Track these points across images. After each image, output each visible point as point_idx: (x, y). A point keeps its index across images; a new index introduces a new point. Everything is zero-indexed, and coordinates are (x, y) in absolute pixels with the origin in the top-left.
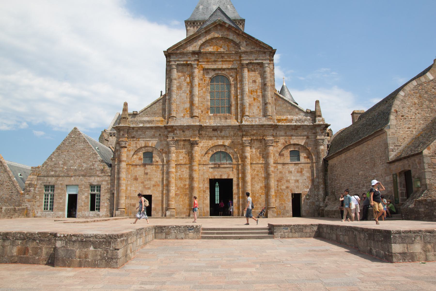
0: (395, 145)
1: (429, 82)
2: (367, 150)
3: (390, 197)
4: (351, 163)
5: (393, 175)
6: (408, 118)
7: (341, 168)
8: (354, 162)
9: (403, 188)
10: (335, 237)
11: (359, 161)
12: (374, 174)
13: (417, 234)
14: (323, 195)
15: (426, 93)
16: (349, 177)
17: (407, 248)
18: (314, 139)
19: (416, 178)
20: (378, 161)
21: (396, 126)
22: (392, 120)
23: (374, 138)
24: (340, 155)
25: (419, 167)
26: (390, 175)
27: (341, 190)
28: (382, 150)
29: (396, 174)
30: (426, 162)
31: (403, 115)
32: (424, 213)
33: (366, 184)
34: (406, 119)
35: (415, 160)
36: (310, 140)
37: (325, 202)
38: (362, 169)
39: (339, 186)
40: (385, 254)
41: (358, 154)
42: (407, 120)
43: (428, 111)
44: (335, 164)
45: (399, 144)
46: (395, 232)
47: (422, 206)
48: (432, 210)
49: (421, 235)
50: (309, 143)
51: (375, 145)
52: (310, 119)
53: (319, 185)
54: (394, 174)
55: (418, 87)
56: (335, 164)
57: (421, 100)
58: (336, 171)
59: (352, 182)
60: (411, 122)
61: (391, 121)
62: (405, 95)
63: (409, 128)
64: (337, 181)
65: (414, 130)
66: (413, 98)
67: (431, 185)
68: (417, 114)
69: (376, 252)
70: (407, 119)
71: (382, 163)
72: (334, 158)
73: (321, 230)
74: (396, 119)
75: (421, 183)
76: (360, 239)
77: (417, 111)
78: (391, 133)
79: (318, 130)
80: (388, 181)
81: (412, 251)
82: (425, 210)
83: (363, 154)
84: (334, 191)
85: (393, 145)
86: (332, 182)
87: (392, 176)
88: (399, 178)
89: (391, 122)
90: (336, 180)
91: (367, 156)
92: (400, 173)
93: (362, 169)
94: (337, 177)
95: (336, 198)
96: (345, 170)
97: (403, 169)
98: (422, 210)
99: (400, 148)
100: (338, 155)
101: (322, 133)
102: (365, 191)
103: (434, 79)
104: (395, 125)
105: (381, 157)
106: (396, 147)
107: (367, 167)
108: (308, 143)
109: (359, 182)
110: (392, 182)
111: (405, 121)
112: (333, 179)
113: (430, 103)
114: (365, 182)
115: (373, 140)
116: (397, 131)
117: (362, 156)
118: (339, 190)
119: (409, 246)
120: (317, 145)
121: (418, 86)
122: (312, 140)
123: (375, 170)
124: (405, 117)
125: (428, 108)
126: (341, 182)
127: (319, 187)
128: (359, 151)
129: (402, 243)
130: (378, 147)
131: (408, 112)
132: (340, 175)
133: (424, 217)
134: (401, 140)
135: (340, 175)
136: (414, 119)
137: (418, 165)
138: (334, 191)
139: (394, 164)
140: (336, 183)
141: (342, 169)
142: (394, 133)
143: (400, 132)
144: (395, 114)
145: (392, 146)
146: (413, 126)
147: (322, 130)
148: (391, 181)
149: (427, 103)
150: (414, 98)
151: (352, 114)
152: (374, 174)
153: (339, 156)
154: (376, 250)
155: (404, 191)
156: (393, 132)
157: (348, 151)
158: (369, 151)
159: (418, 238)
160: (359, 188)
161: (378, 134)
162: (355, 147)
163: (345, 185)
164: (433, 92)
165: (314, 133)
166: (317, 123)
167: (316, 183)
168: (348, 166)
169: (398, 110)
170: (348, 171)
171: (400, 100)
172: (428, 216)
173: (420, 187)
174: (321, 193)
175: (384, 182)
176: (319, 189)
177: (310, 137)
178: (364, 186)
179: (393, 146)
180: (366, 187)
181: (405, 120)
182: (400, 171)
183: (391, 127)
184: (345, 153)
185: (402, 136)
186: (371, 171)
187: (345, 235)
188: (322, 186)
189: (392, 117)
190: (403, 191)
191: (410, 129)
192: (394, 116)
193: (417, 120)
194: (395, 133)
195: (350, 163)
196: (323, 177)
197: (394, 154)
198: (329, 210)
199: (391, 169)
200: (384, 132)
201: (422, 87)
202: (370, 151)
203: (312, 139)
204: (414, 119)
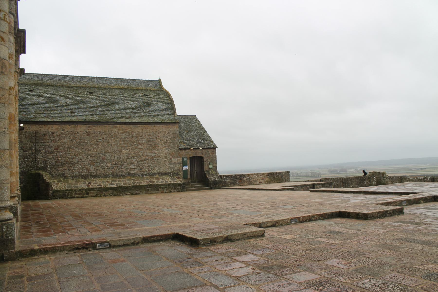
5: (183, 159)
26: (179, 158)
35: (208, 151)
48: (236, 180)
97: (195, 155)
98: (229, 181)
114: (135, 160)
123: (155, 152)
130: (162, 134)
133: (229, 185)
137: (211, 154)
148: (180, 162)
160: (122, 165)
175: (169, 162)
178: (132, 163)
182: (192, 156)
187: (301, 189)
199: (181, 153)
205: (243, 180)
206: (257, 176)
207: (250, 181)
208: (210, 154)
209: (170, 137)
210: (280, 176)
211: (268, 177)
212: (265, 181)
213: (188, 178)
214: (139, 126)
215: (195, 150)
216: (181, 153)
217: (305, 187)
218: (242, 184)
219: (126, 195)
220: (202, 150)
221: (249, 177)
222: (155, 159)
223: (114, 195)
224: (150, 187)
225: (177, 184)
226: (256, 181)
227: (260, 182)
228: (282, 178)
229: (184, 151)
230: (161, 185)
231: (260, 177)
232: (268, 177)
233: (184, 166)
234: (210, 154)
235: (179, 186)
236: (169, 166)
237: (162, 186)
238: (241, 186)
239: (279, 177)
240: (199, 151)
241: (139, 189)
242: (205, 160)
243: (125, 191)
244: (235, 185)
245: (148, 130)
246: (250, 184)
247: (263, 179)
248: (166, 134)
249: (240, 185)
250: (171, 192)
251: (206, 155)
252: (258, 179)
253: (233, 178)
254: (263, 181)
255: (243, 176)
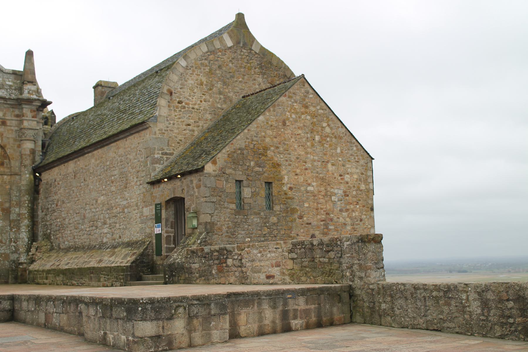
0: (163, 151)
1: (226, 49)
2: (115, 157)
3: (148, 244)
4: (84, 180)
5: (156, 205)
6: (187, 108)
7: (66, 189)
8: (91, 178)
9: (170, 229)
10: (44, 317)
11: (99, 177)
12: (125, 203)
13: (179, 304)
14: (27, 240)
15: (220, 67)
16: (79, 206)
17: (163, 328)
18: (16, 128)
19: (192, 211)
20: (133, 178)
21: (168, 119)
22: (162, 108)
23: (128, 136)
24: (66, 164)
25: (197, 194)
26: (151, 205)
27: (63, 231)
28: (141, 160)
29: (160, 204)
30: (209, 186)
31: (181, 101)
32: (199, 270)
33: (109, 220)
34: (184, 107)
35: (192, 181)
36: (9, 128)
37: (30, 253)
38: (104, 192)
39: (59, 224)
40: (128, 340)
41: (98, 164)
42: (186, 111)
43: (220, 99)
44: (55, 181)
45: (170, 150)
46: (145, 302)
47: (197, 260)
48: (210, 266)
49: (185, 304)
50: (4, 135)
51: (129, 149)
52: (10, 86)
53: (19, 220)
54: (158, 204)
55: (209, 55)
56: (55, 181)
57: (211, 79)
58: (56, 193)
59: (84, 216)
60: (192, 115)
61: (160, 108)
62: (187, 66)
63: (189, 125)
64: (56, 214)
65: (195, 129)
66: (199, 73)
67: (213, 223)
68: (203, 102)
69: (114, 338)
70: (187, 109)
71: (138, 183)
72: (54, 169)
73: (17, 306)
74: (169, 106)
75: (198, 220)
76: (89, 317)
77: (204, 97)
78: (159, 130)
79: (27, 110)
80: (147, 216)
81: (169, 333)
82: (200, 267)
83: (108, 163)
84: (50, 233)
85: (160, 152)
86: (46, 215)
87: (154, 206)
88: (165, 212)
89: (159, 111)
90: (54, 211)
91: (114, 168)
92: (168, 202)
93: (104, 192)
94: (57, 205)
95: (52, 246)
96: (74, 193)
97: (173, 196)
98: (197, 266)
99: (172, 157)
100: (62, 164)
101: (33, 117)
102: (106, 233)
103: (234, 46)
104: (167, 117)
105: (138, 172)
106: (165, 156)
107: (113, 189)
108: (2, 135)
109: (97, 217)
110: (154, 217)
111: (183, 111)
112: (48, 209)
113: (223, 86)
114: (107, 216)
115: (126, 141)
116: (168, 127)
117: (105, 168)
118: (59, 230)
119: (165, 324)
120: (21, 140)
121: (209, 53)
122: (12, 130)
123: (127, 195)
124: (183, 104)
125: (220, 93)
126: (63, 216)
127: (19, 224)
128: (102, 158)
129: (155, 319)
130: (134, 154)
131: (190, 96)
132: (63, 202)
133: (197, 278)
134: (173, 145)
135: (63, 202)
136: (198, 110)
137: (196, 190)
138: (50, 233)
139: (159, 187)
140: (53, 218)
141: (67, 191)
142: (163, 131)
143: (173, 131)
144: (168, 97)
145: (158, 153)
146: (195, 122)
147: (34, 111)
148: (153, 215)
149: (219, 85)
150: (201, 74)
151: (95, 88)
152: (125, 203)
153: (63, 165)
154: (113, 334)
155: (172, 235)
156: (162, 130)
157: (80, 156)
158: (119, 159)
159: (181, 310)
161: (137, 130)
162: (94, 151)
163: (71, 222)
164: (230, 68)
165: (17, 116)
166: (26, 95)
167: (15, 216)
168: (79, 185)
169: (173, 92)
170: (78, 194)
171: (179, 74)
172: (203, 276)
173: (197, 228)
174: (24, 236)
175: (140, 217)
176: (19, 228)
177: (8, 123)
178: (105, 223)
179: (160, 154)
180: (108, 226)
181: (182, 110)
182: (168, 198)
183: (159, 119)
184: (74, 160)
185: (176, 137)
186: (119, 197)
187: (63, 313)
188: (26, 222)
189: (162, 102)
190: (170, 234)
191: (190, 127)
192: (166, 101)
193: (202, 113)
194: (165, 130)
195: (83, 180)
196: (30, 205)
197: (160, 169)
198: (36, 269)
199: (154, 194)
200: (147, 128)
201: (215, 57)
202: (120, 159)
203: (12, 128)
204: (198, 110)
205: (227, 266)
206: (260, 252)
207: (244, 269)
208: (195, 188)
209: (142, 158)
210: (332, 254)
211: (293, 259)
212: (283, 274)
213: (162, 255)
214: (112, 146)
215: (172, 181)
216: (154, 194)
217: (73, 307)
218: (223, 280)
219: (73, 285)
220: (183, 179)
221: (240, 254)
222: (126, 210)
223: (64, 284)
224: (92, 273)
225: (120, 268)
226: (259, 272)
227: (268, 277)
228: (340, 263)
229: (157, 189)
230: (103, 269)
231: (269, 255)
232: (293, 259)
233: (156, 225)
234: (195, 188)
235: (122, 274)
236: (140, 225)
237: (104, 272)
238: (220, 284)
239: (329, 259)
240: (177, 183)
241: (84, 276)
242: (188, 207)
243: (71, 279)
244: (208, 280)
245: (121, 151)
246: (243, 281)
247: (278, 265)
248: (138, 151)
249: (219, 281)
250: (112, 286)
251: (188, 192)
252: (262, 264)
253: (205, 257)
254: (275, 271)
255: (225, 252)
